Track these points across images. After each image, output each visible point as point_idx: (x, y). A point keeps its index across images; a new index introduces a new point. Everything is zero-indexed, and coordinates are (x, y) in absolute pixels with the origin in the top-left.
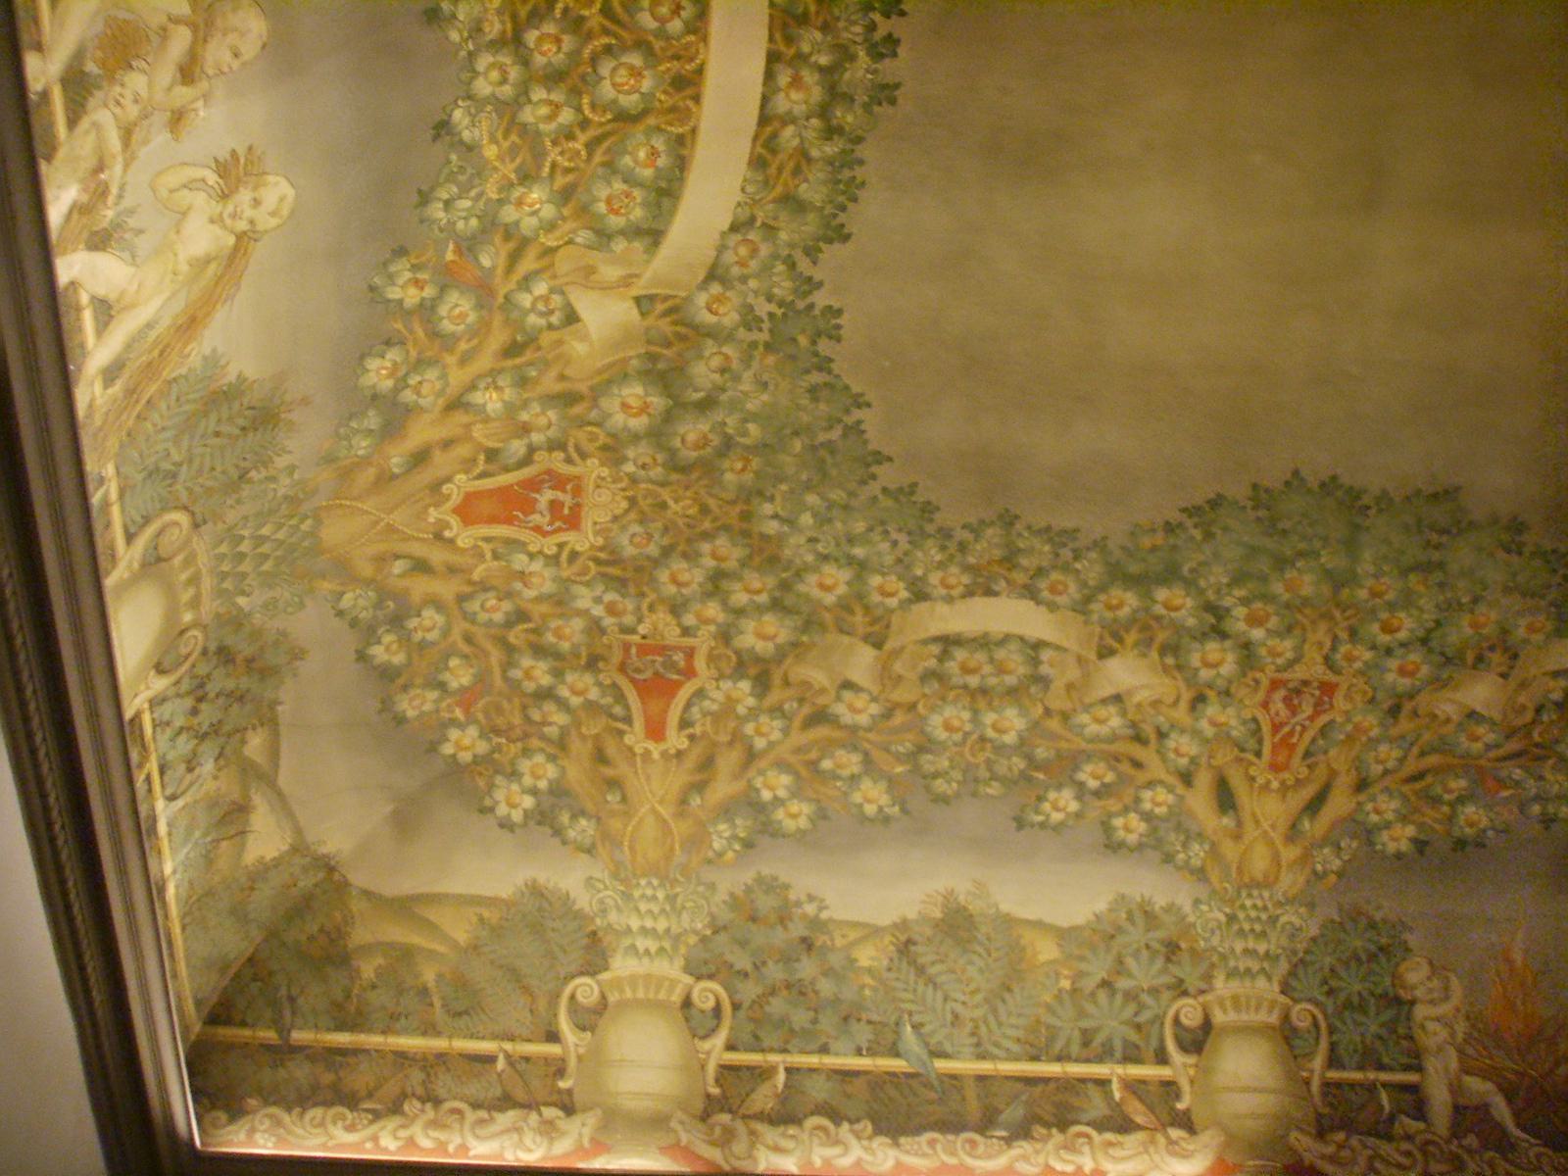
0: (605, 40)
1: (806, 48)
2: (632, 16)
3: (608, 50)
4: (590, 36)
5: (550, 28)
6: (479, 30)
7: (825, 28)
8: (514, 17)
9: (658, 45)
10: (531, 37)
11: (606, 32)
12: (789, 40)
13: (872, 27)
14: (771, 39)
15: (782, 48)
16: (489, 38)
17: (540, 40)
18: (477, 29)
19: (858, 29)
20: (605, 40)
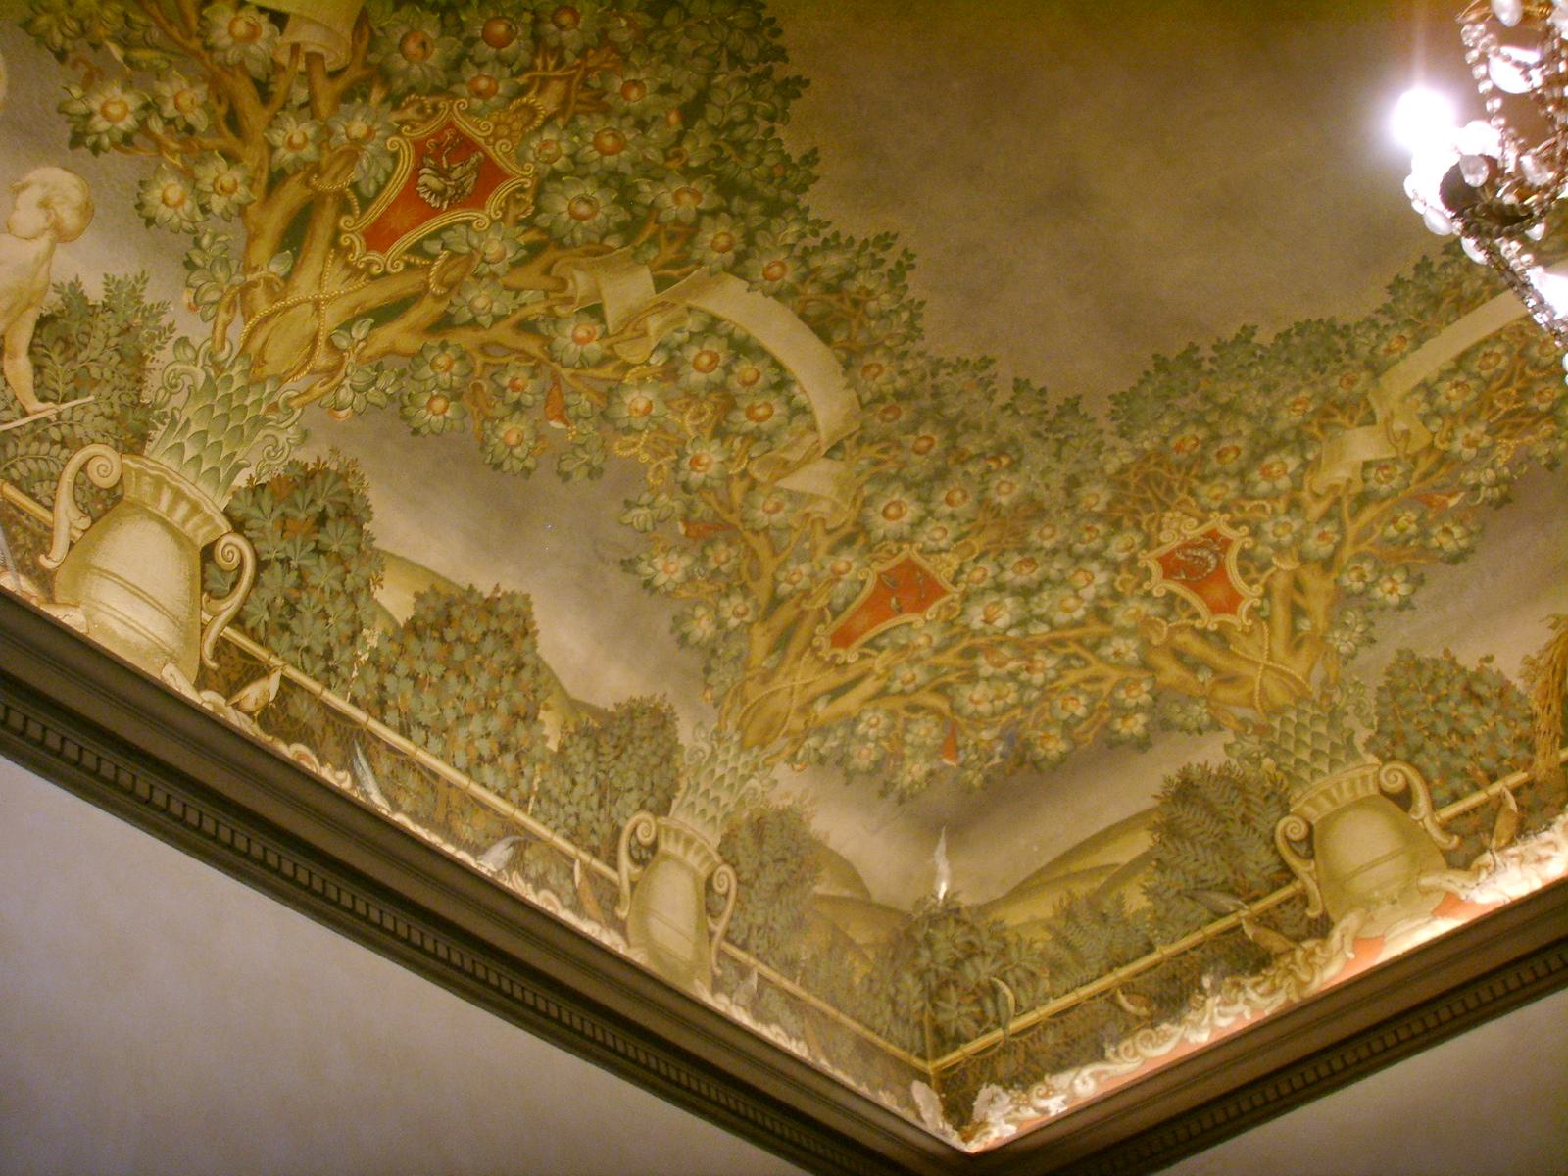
0: (1528, 372)
1: (1480, 282)
2: (1503, 371)
3: (1535, 366)
4: (1531, 381)
5: (1534, 402)
6: (1553, 436)
7: (1458, 285)
8: (1535, 423)
9: (1517, 347)
10: (1543, 407)
11: (1522, 374)
12: (1477, 294)
13: (1445, 265)
14: (1483, 302)
15: (1485, 294)
16: (1555, 428)
17: (1541, 401)
18: (1554, 437)
19: (1450, 271)
20: (1528, 372)
